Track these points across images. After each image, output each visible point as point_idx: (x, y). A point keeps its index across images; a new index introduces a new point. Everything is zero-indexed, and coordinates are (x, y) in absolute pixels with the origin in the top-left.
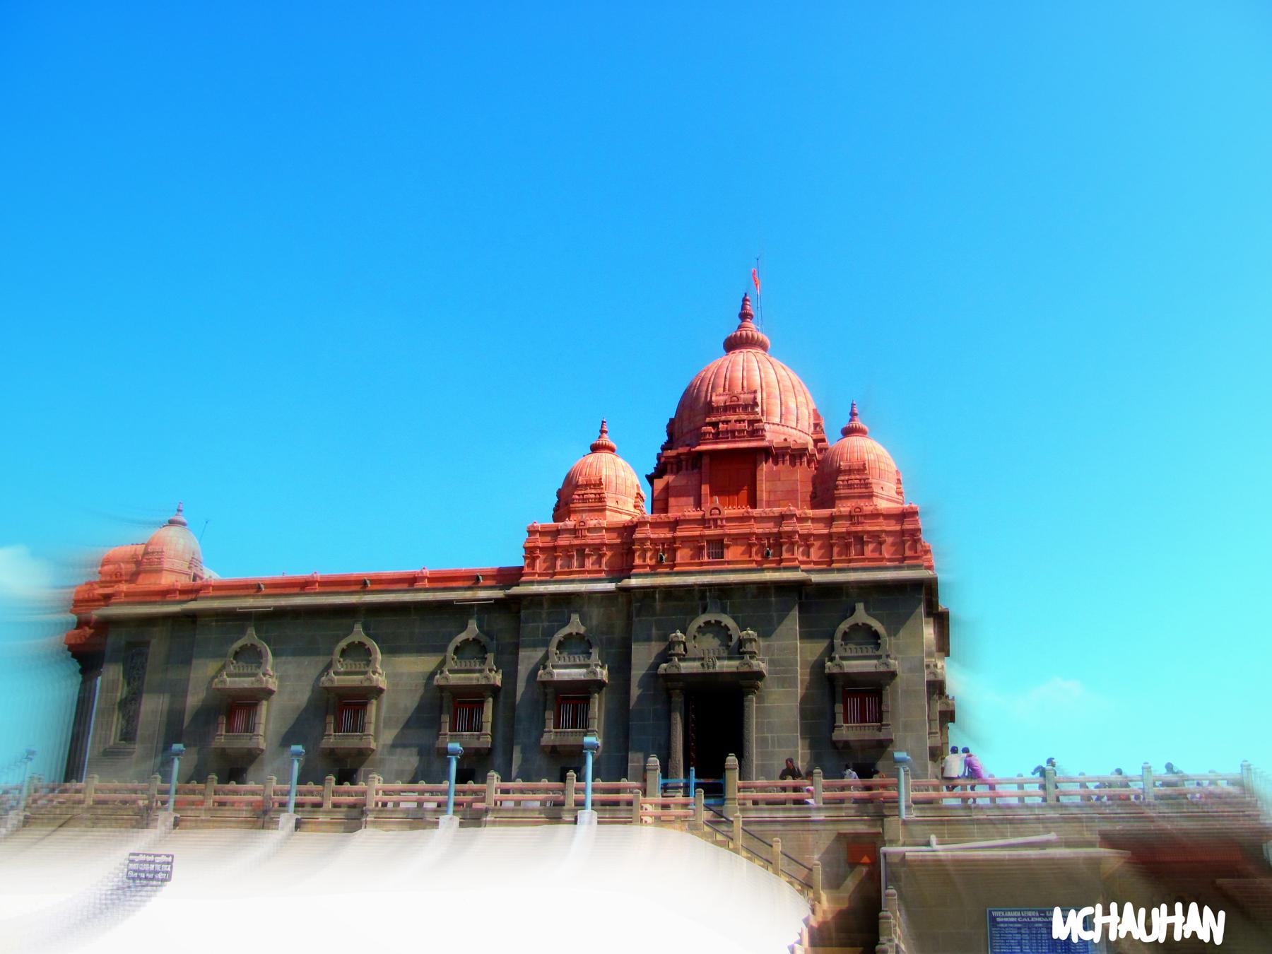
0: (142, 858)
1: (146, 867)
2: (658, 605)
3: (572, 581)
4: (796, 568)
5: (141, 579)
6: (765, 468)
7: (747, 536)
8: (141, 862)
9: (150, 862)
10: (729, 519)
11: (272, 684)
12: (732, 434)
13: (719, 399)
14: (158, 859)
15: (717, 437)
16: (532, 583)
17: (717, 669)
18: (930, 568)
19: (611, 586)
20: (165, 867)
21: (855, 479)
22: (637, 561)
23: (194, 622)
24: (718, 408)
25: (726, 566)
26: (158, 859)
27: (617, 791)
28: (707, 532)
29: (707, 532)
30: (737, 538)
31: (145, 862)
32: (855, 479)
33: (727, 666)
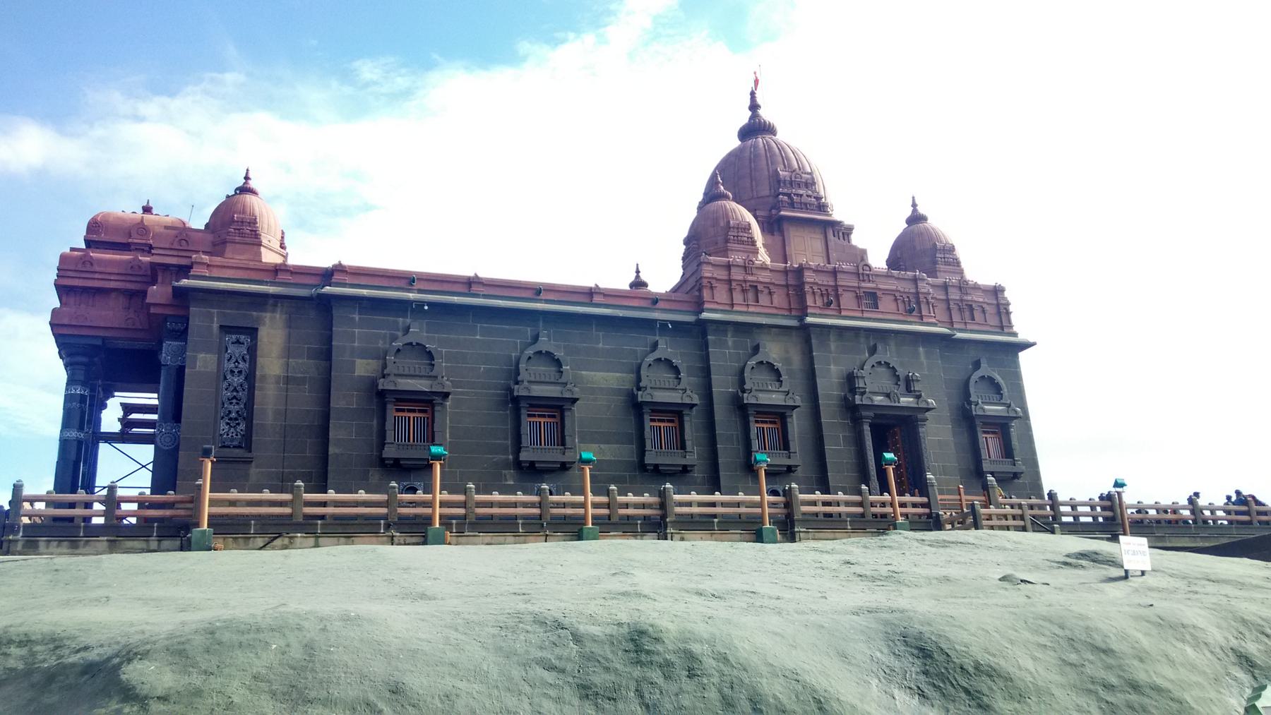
12: (805, 207)
28: (863, 285)
29: (863, 285)
30: (887, 292)
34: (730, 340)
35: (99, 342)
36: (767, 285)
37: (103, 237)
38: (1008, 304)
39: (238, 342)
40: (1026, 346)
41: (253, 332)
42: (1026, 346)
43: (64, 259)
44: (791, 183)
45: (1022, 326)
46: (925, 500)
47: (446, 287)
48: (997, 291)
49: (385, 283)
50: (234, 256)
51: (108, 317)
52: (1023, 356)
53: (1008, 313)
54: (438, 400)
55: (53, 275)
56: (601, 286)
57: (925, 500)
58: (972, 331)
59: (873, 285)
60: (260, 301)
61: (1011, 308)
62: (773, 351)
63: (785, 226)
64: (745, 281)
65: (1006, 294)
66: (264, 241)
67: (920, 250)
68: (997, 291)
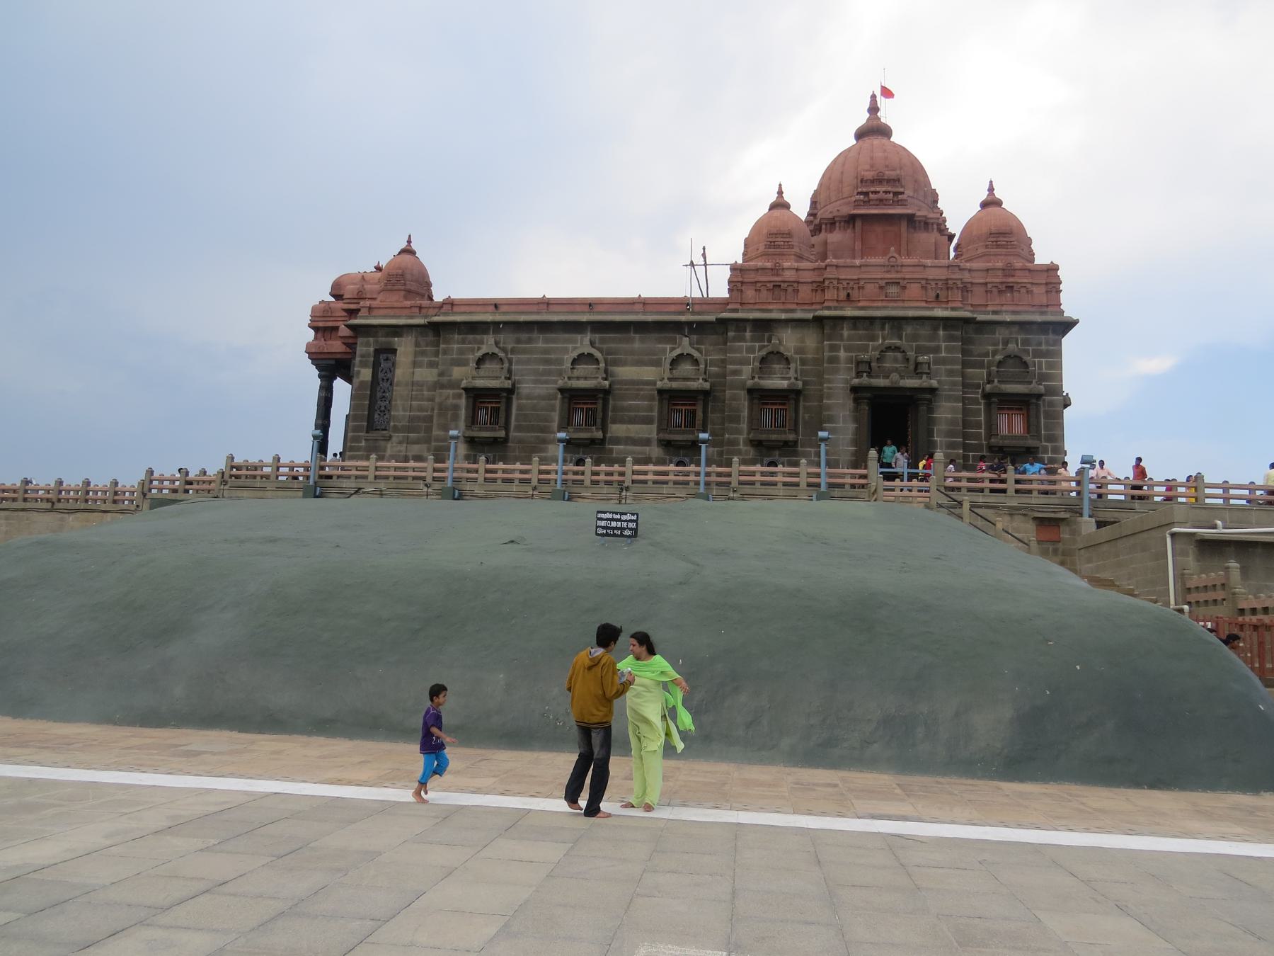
0: (610, 516)
1: (614, 524)
2: (846, 333)
8: (608, 519)
9: (617, 520)
12: (881, 202)
14: (624, 517)
20: (630, 525)
26: (624, 517)
31: (613, 520)
34: (748, 334)
35: (333, 362)
39: (387, 359)
41: (394, 351)
42: (1069, 325)
43: (314, 309)
44: (873, 181)
45: (1070, 305)
47: (522, 308)
48: (1052, 269)
49: (479, 309)
55: (308, 320)
59: (899, 276)
60: (396, 330)
62: (788, 340)
65: (1059, 273)
68: (1052, 269)
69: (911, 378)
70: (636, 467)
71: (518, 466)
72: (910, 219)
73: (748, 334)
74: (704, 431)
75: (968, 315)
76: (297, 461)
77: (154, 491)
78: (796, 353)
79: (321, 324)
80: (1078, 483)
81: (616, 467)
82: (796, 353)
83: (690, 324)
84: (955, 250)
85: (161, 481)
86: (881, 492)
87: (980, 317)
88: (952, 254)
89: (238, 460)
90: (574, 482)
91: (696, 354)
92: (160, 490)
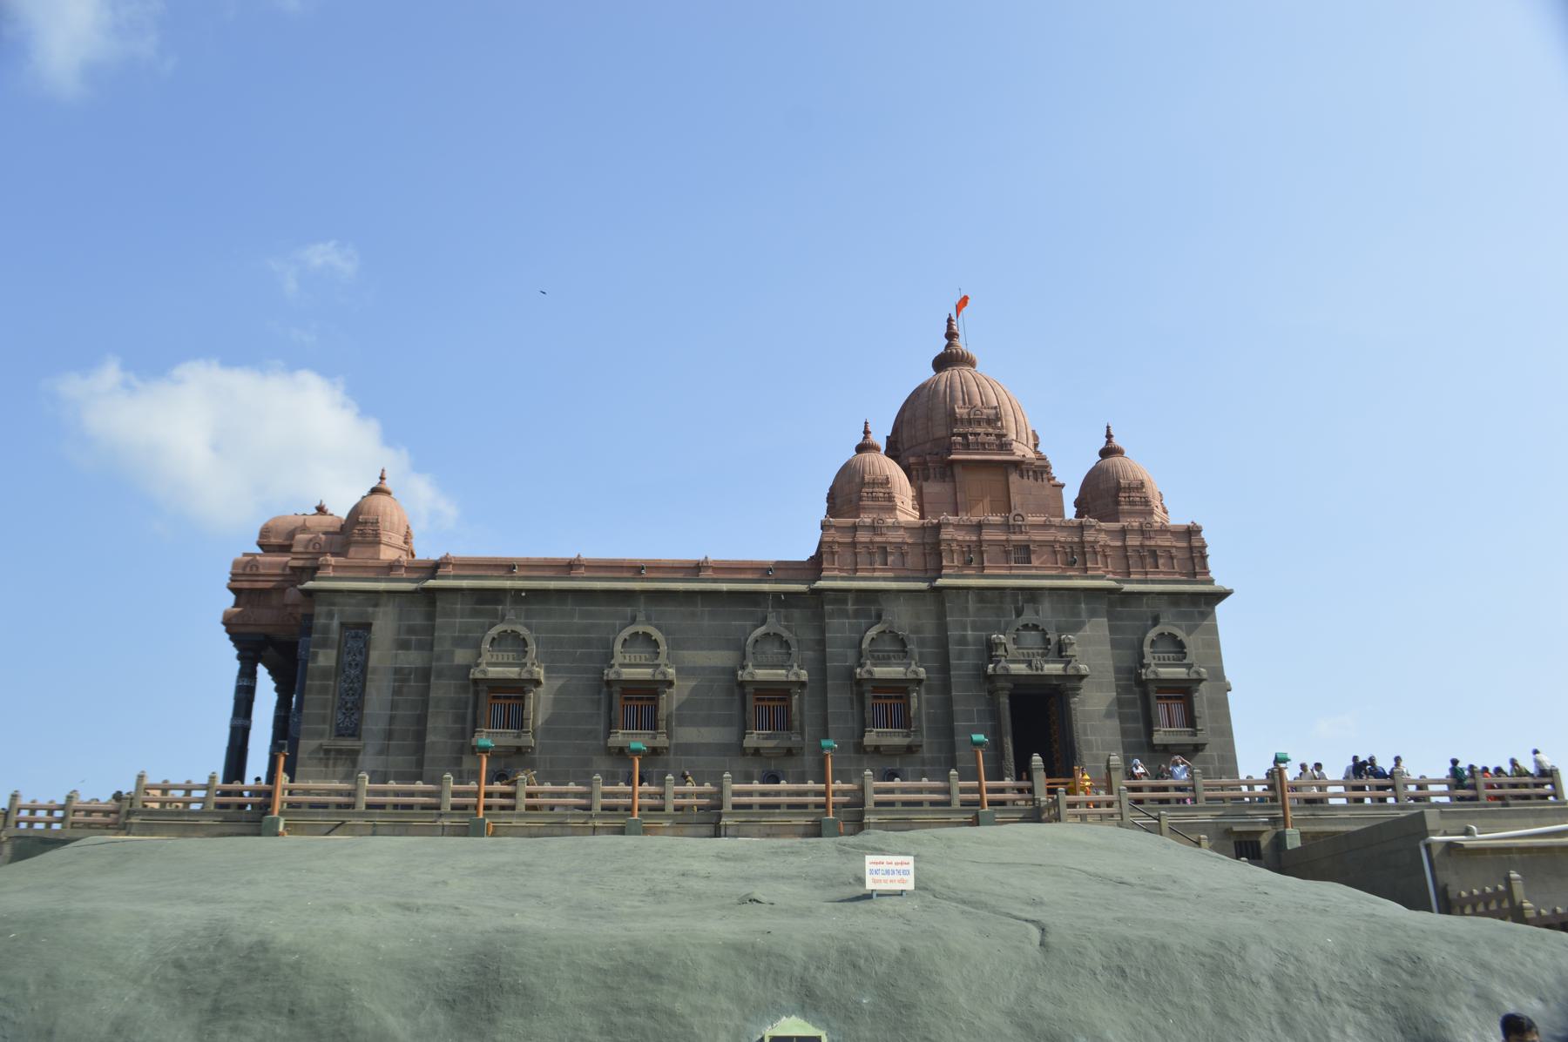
3: (877, 579)
4: (1102, 577)
5: (352, 551)
6: (1014, 478)
7: (1051, 544)
10: (1034, 526)
11: (540, 673)
12: (983, 447)
13: (960, 411)
15: (966, 446)
16: (834, 578)
17: (1046, 672)
18: (1211, 582)
19: (923, 585)
21: (1135, 496)
22: (944, 563)
23: (432, 603)
24: (962, 420)
25: (1034, 572)
27: (891, 791)
28: (1014, 537)
29: (1014, 537)
30: (1042, 544)
32: (1135, 496)
33: (1053, 668)
34: (850, 607)
36: (899, 546)
37: (273, 541)
38: (1204, 547)
40: (1222, 595)
41: (368, 627)
42: (1222, 595)
43: (236, 564)
46: (1028, 784)
48: (1192, 532)
50: (357, 555)
51: (265, 618)
52: (1220, 609)
53: (1204, 557)
54: (528, 687)
56: (711, 558)
57: (1028, 784)
58: (1153, 582)
61: (1208, 551)
62: (901, 618)
63: (958, 470)
64: (872, 542)
66: (384, 539)
67: (1108, 492)
68: (1192, 532)
69: (1054, 662)
70: (737, 787)
71: (572, 787)
72: (1018, 465)
73: (850, 607)
74: (827, 738)
75: (1112, 584)
76: (173, 781)
77: (23, 825)
78: (912, 632)
79: (246, 585)
80: (1272, 787)
81: (708, 787)
82: (912, 632)
83: (776, 594)
84: (1077, 503)
85: (33, 811)
86: (1065, 811)
87: (1127, 587)
88: (1070, 512)
89: (153, 778)
90: (652, 809)
91: (786, 634)
92: (31, 824)
